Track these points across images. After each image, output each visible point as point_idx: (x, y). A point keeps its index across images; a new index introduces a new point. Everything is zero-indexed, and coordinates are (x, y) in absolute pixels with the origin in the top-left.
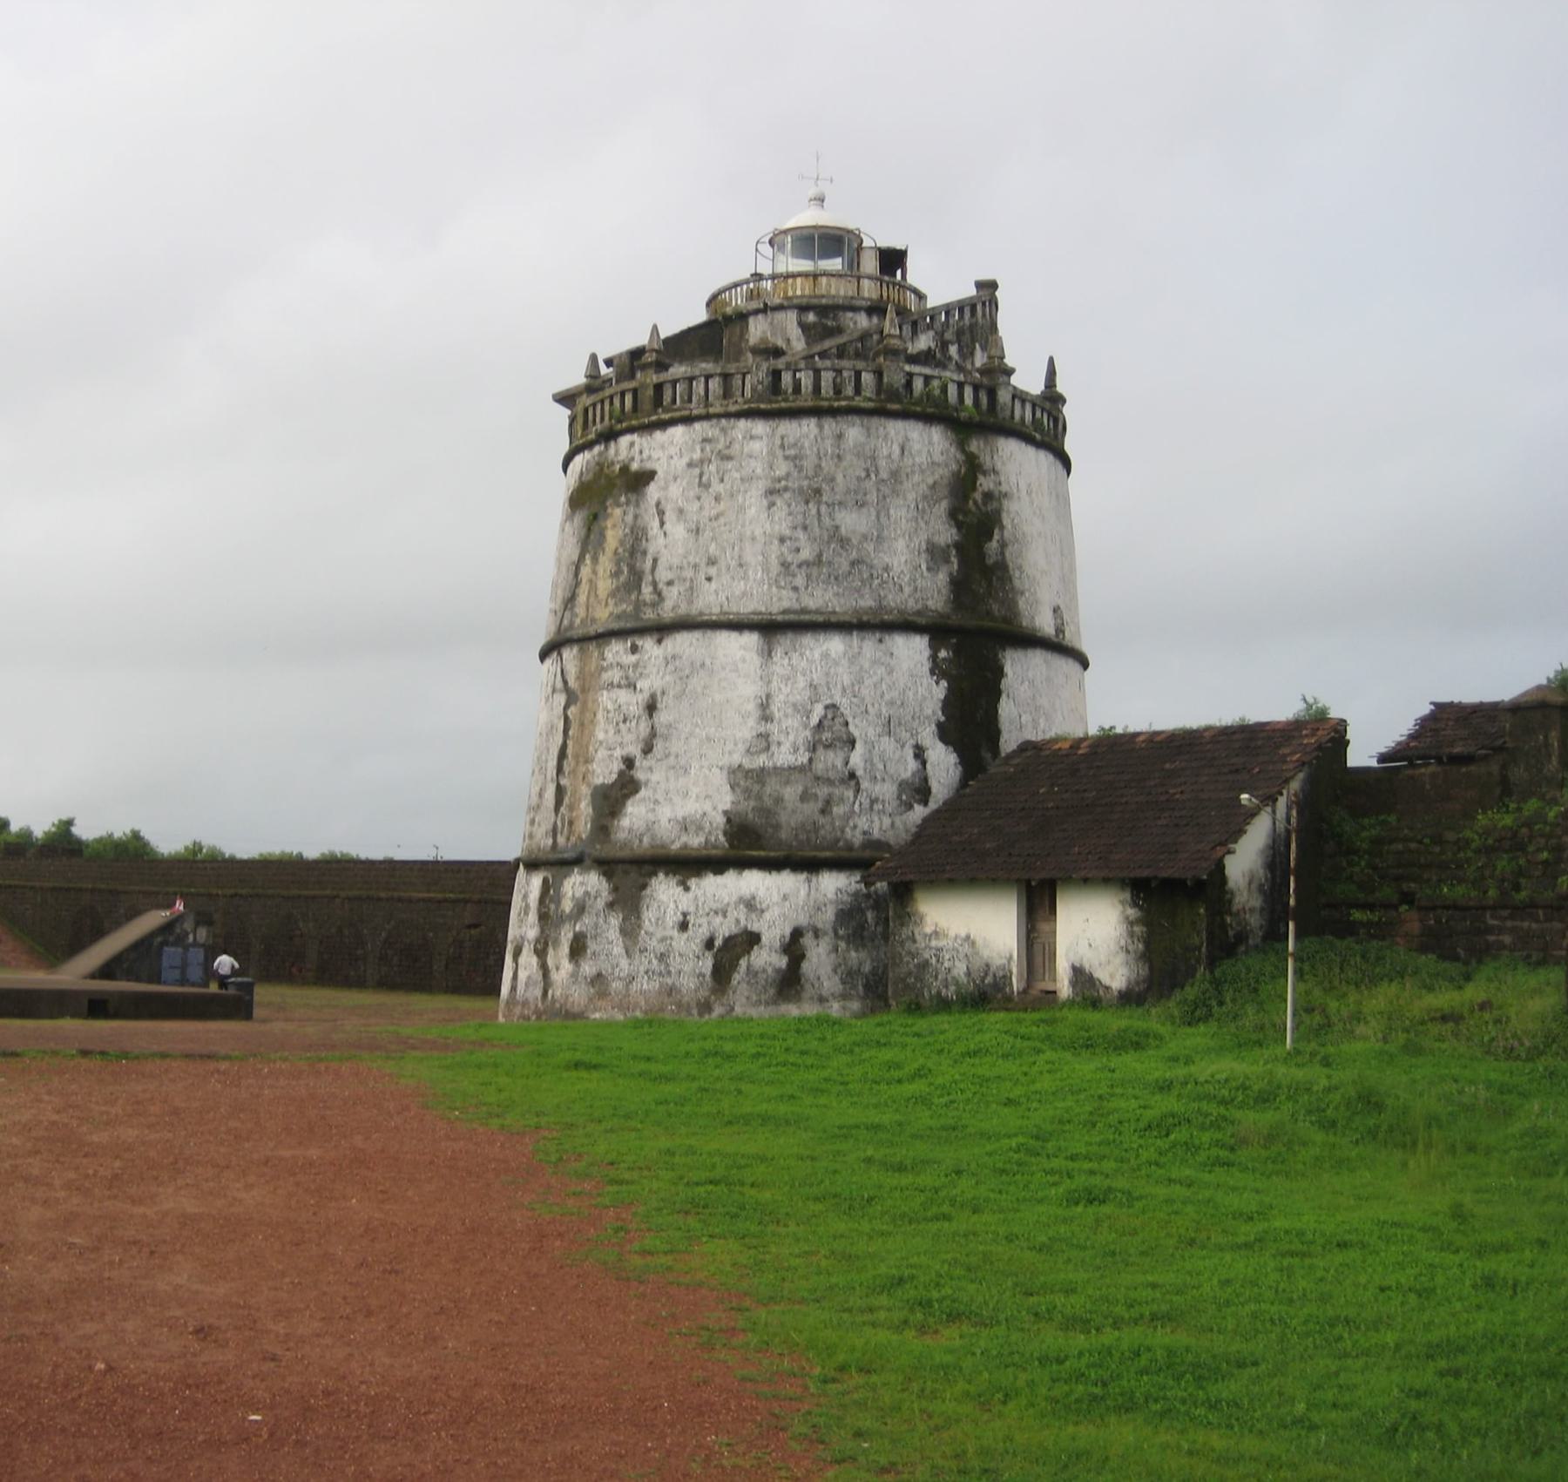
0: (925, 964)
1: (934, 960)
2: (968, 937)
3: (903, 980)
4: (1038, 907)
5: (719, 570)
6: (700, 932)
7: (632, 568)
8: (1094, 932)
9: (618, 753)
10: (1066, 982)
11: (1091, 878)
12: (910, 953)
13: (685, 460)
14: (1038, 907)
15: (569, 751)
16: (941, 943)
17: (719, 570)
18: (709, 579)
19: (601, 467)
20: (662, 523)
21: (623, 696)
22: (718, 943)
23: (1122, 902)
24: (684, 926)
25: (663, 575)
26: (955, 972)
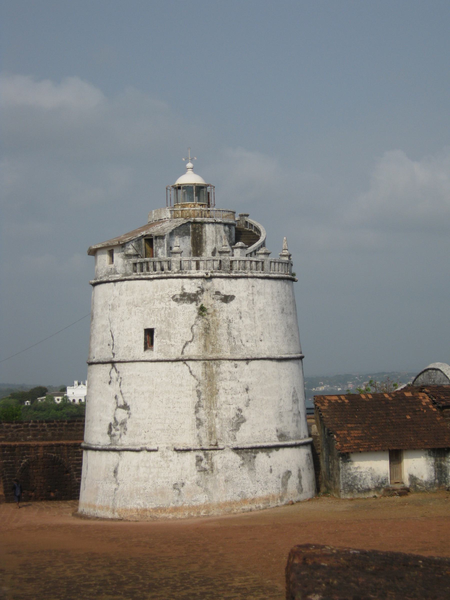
0: (355, 478)
1: (359, 476)
2: (371, 468)
3: (347, 483)
4: (395, 457)
5: (264, 338)
6: (275, 473)
7: (229, 334)
9: (234, 406)
10: (407, 479)
11: (414, 448)
12: (349, 474)
13: (246, 293)
14: (395, 457)
15: (204, 403)
16: (361, 470)
17: (264, 338)
18: (261, 341)
20: (241, 318)
21: (233, 384)
22: (281, 476)
23: (426, 455)
24: (271, 471)
25: (244, 339)
26: (367, 480)
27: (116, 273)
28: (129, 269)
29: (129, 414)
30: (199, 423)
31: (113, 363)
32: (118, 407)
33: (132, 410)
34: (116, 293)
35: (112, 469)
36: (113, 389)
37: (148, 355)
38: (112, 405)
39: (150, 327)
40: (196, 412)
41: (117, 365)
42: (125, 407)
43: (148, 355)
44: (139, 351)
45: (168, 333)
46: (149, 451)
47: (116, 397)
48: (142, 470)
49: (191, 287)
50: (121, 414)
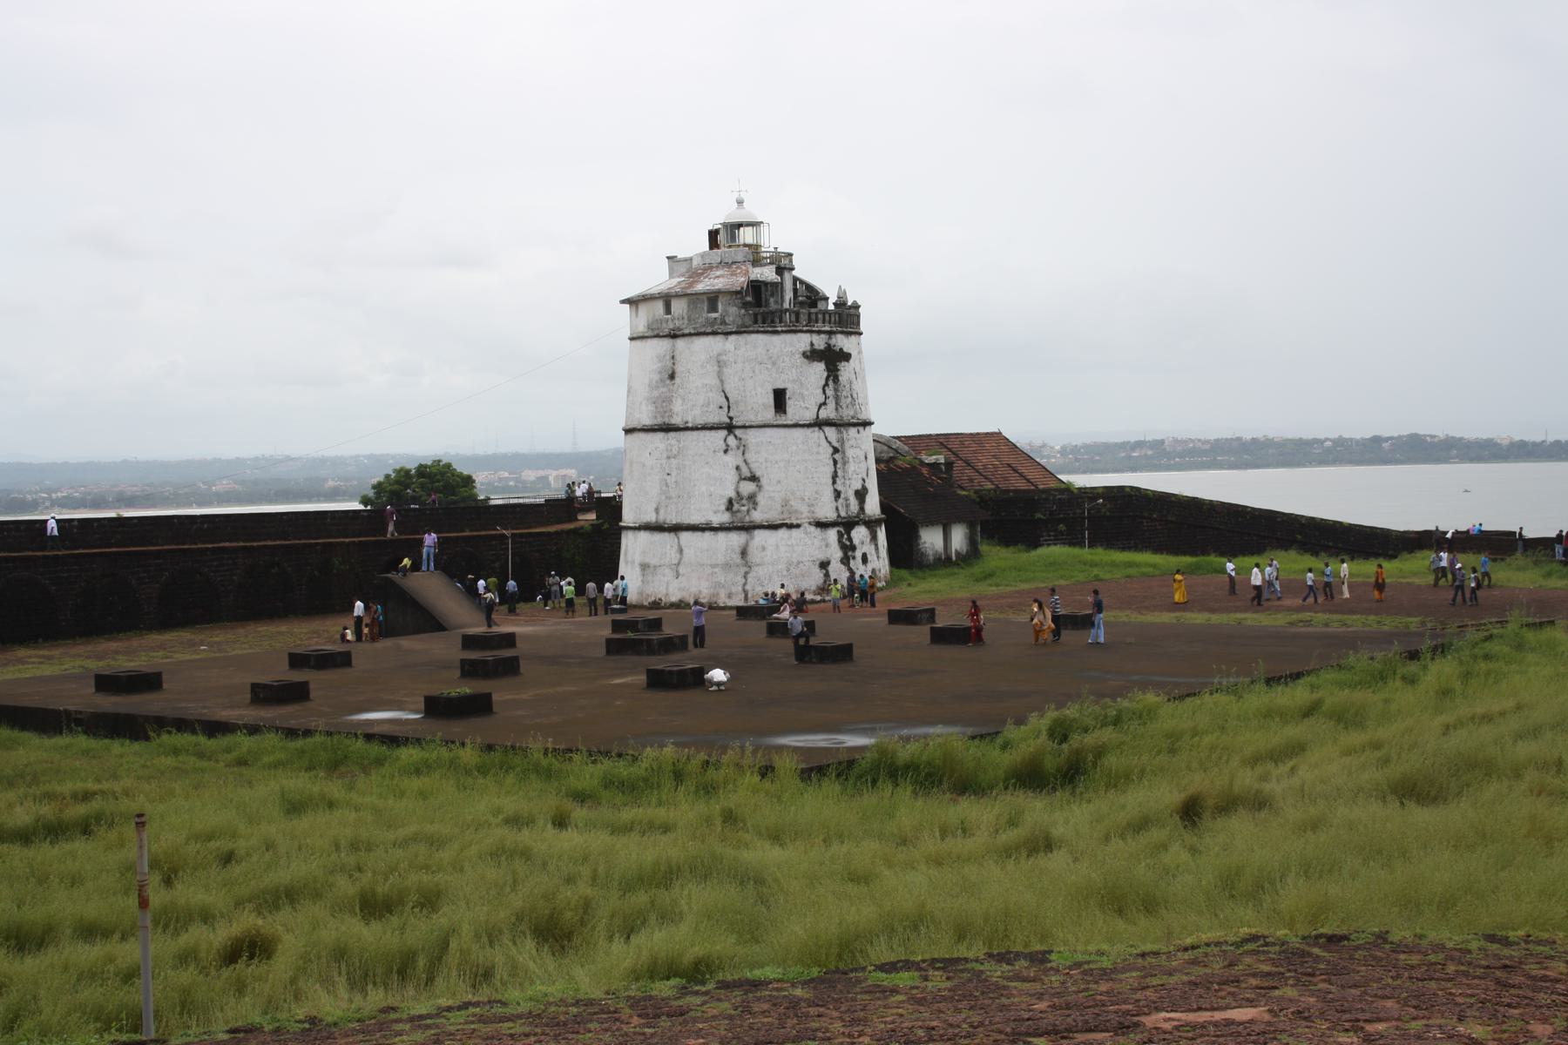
8: (959, 538)
19: (829, 347)
27: (723, 323)
28: (748, 321)
29: (760, 487)
30: (837, 494)
31: (730, 428)
32: (742, 479)
33: (764, 481)
35: (738, 550)
36: (732, 459)
37: (782, 420)
38: (732, 477)
39: (781, 386)
40: (834, 482)
41: (738, 432)
42: (753, 478)
43: (782, 420)
44: (769, 414)
45: (802, 395)
46: (791, 526)
47: (738, 468)
48: (782, 549)
49: (820, 342)
50: (748, 488)
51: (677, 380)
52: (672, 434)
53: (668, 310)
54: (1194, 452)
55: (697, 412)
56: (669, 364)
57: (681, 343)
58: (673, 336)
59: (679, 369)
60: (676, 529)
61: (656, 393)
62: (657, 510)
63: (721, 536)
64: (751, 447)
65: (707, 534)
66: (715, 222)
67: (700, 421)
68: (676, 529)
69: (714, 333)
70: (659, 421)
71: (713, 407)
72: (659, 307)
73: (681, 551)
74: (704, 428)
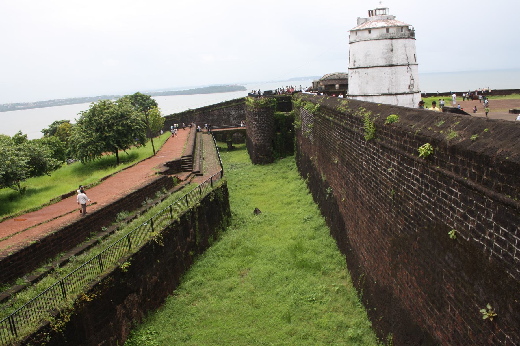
31: (408, 65)
34: (407, 42)
36: (409, 74)
38: (409, 79)
42: (413, 79)
51: (394, 51)
52: (393, 67)
53: (388, 30)
54: (61, 102)
55: (400, 60)
56: (391, 47)
57: (394, 41)
58: (392, 38)
59: (394, 48)
60: (396, 94)
61: (386, 56)
62: (388, 89)
63: (408, 95)
64: (412, 71)
65: (405, 95)
66: (372, 8)
67: (401, 63)
68: (396, 94)
69: (404, 38)
70: (388, 63)
71: (404, 59)
72: (385, 30)
73: (398, 101)
74: (403, 65)
